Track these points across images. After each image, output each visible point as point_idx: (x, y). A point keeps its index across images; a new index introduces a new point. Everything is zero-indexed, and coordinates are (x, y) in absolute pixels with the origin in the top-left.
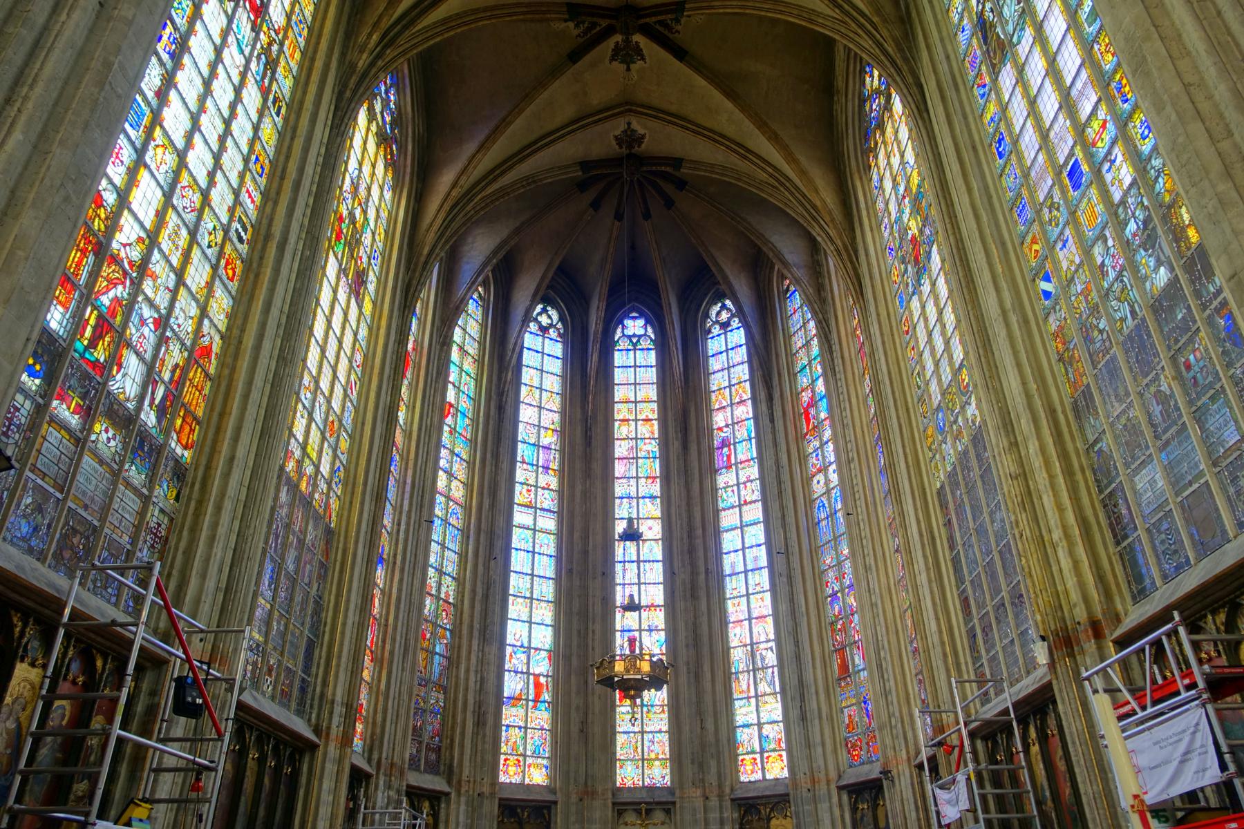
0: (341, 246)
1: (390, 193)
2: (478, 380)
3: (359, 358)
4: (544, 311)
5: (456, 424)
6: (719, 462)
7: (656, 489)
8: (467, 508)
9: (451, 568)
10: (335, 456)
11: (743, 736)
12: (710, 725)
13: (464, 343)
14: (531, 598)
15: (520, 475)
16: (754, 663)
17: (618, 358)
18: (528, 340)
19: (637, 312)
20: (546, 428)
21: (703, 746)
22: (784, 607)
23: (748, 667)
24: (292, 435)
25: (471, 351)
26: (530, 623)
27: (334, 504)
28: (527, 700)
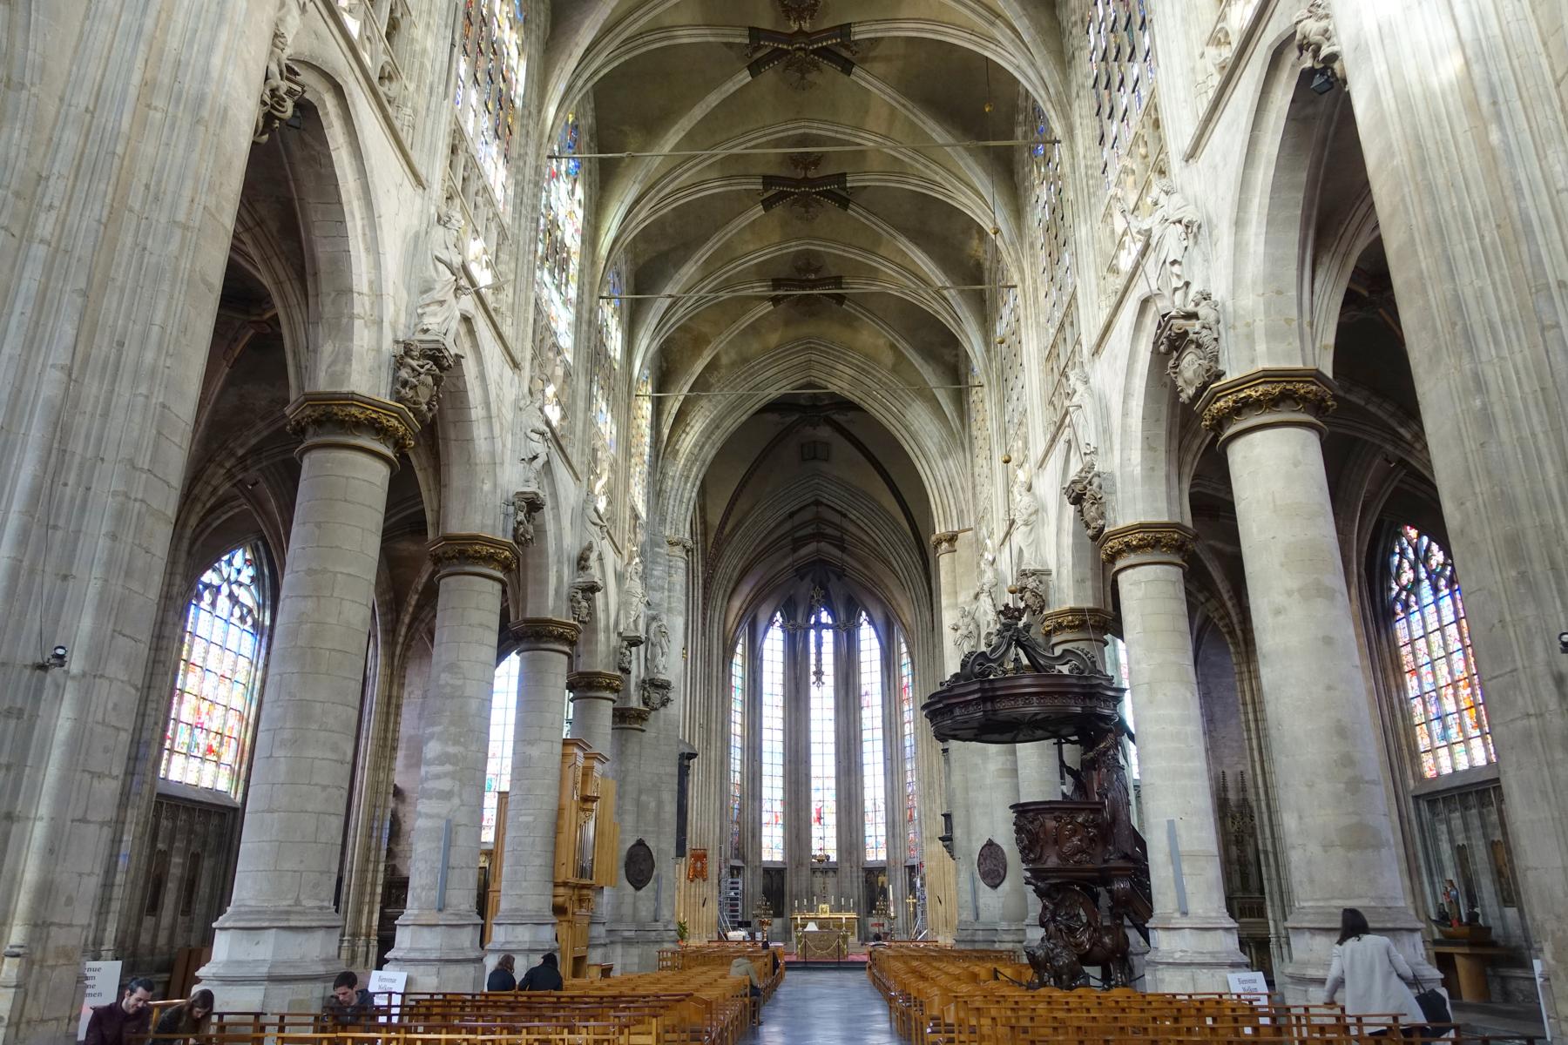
2: (743, 667)
6: (864, 703)
7: (831, 714)
8: (742, 737)
9: (738, 768)
11: (868, 840)
12: (854, 835)
21: (851, 845)
22: (889, 785)
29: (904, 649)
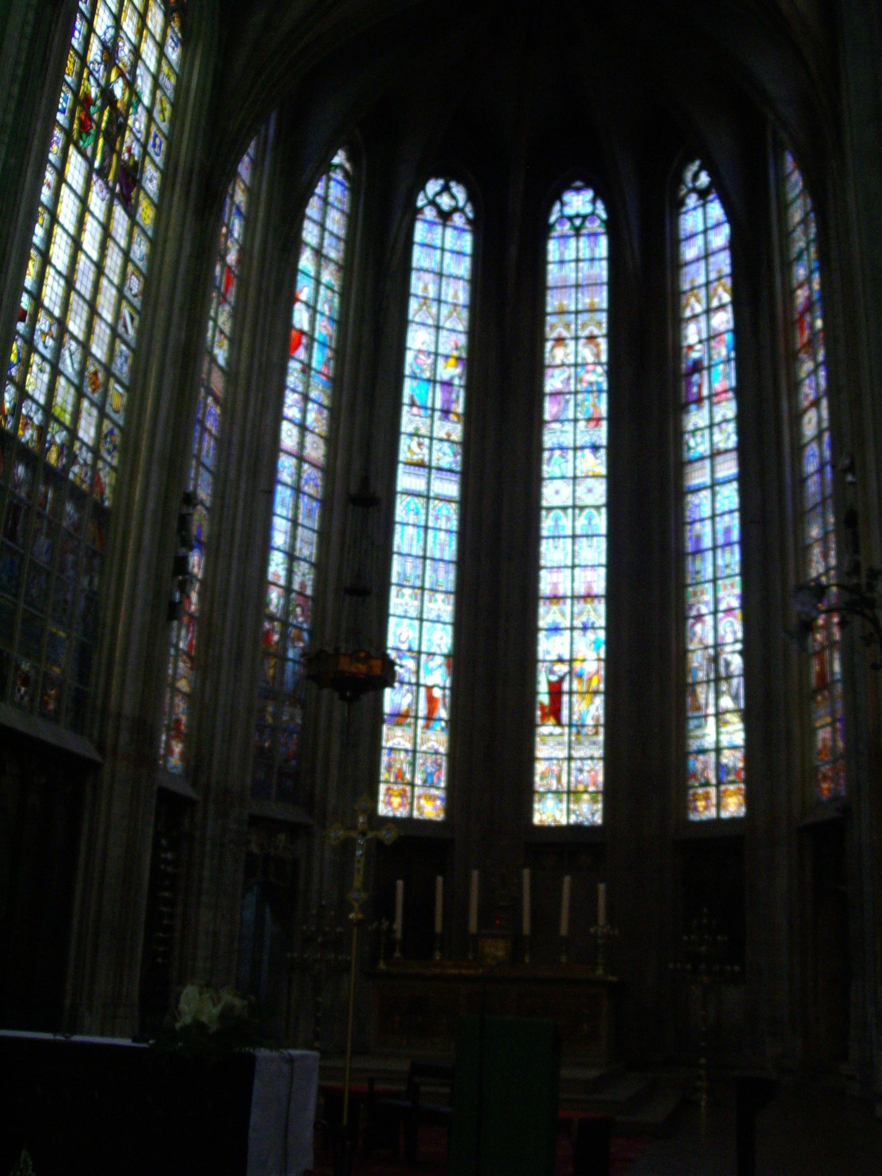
0: (91, 139)
1: (178, 50)
3: (135, 285)
4: (446, 189)
5: (310, 357)
7: (601, 434)
10: (103, 415)
11: (696, 764)
13: (321, 245)
14: (422, 588)
15: (409, 420)
16: (717, 671)
17: (553, 248)
18: (420, 232)
19: (582, 180)
20: (447, 357)
23: (708, 675)
24: (23, 395)
25: (333, 255)
26: (421, 620)
27: (107, 478)
28: (416, 718)
29: (796, 181)
